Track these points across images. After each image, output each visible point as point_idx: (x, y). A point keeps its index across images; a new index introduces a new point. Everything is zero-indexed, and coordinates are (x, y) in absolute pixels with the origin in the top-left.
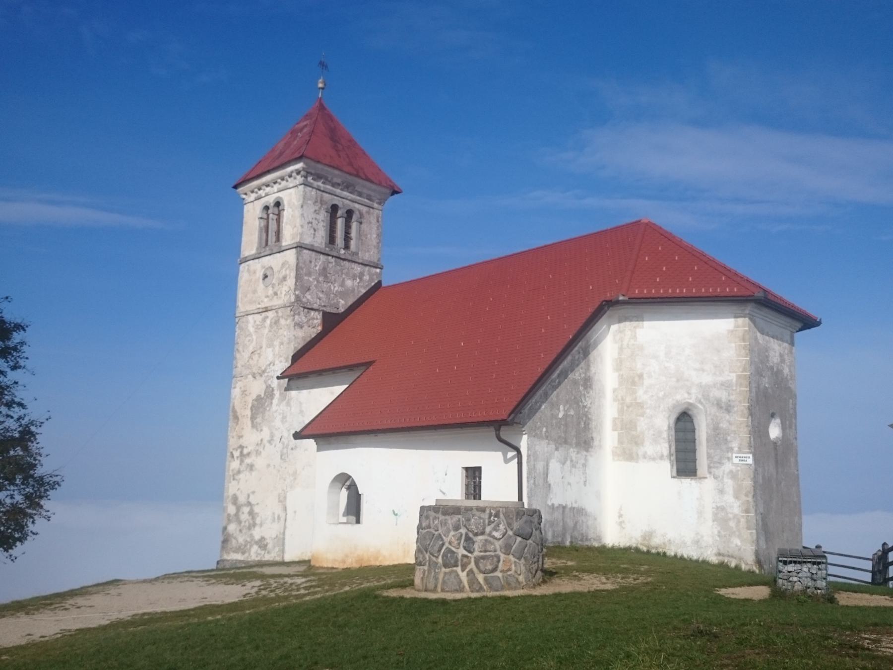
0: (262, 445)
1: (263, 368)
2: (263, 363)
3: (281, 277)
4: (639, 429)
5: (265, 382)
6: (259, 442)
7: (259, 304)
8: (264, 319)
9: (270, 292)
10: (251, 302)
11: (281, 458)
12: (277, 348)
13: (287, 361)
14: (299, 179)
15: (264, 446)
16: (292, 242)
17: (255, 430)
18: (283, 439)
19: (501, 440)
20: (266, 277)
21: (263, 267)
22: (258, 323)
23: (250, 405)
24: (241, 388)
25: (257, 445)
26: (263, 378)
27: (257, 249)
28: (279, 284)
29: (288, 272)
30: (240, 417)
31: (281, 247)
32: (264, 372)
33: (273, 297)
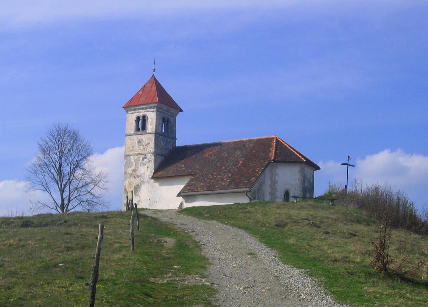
0: (140, 202)
1: (139, 175)
2: (138, 173)
3: (147, 143)
4: (276, 195)
5: (140, 180)
6: (139, 201)
7: (136, 152)
8: (139, 158)
9: (142, 148)
10: (131, 151)
11: (150, 206)
12: (146, 168)
13: (151, 172)
14: (155, 109)
15: (141, 202)
16: (151, 131)
17: (137, 197)
18: (150, 200)
19: (247, 195)
20: (139, 142)
21: (137, 138)
22: (136, 158)
23: (134, 187)
24: (128, 182)
25: (138, 201)
26: (139, 178)
27: (134, 131)
28: (146, 145)
29: (150, 142)
30: (129, 192)
31: (147, 132)
32: (140, 176)
33: (143, 150)
